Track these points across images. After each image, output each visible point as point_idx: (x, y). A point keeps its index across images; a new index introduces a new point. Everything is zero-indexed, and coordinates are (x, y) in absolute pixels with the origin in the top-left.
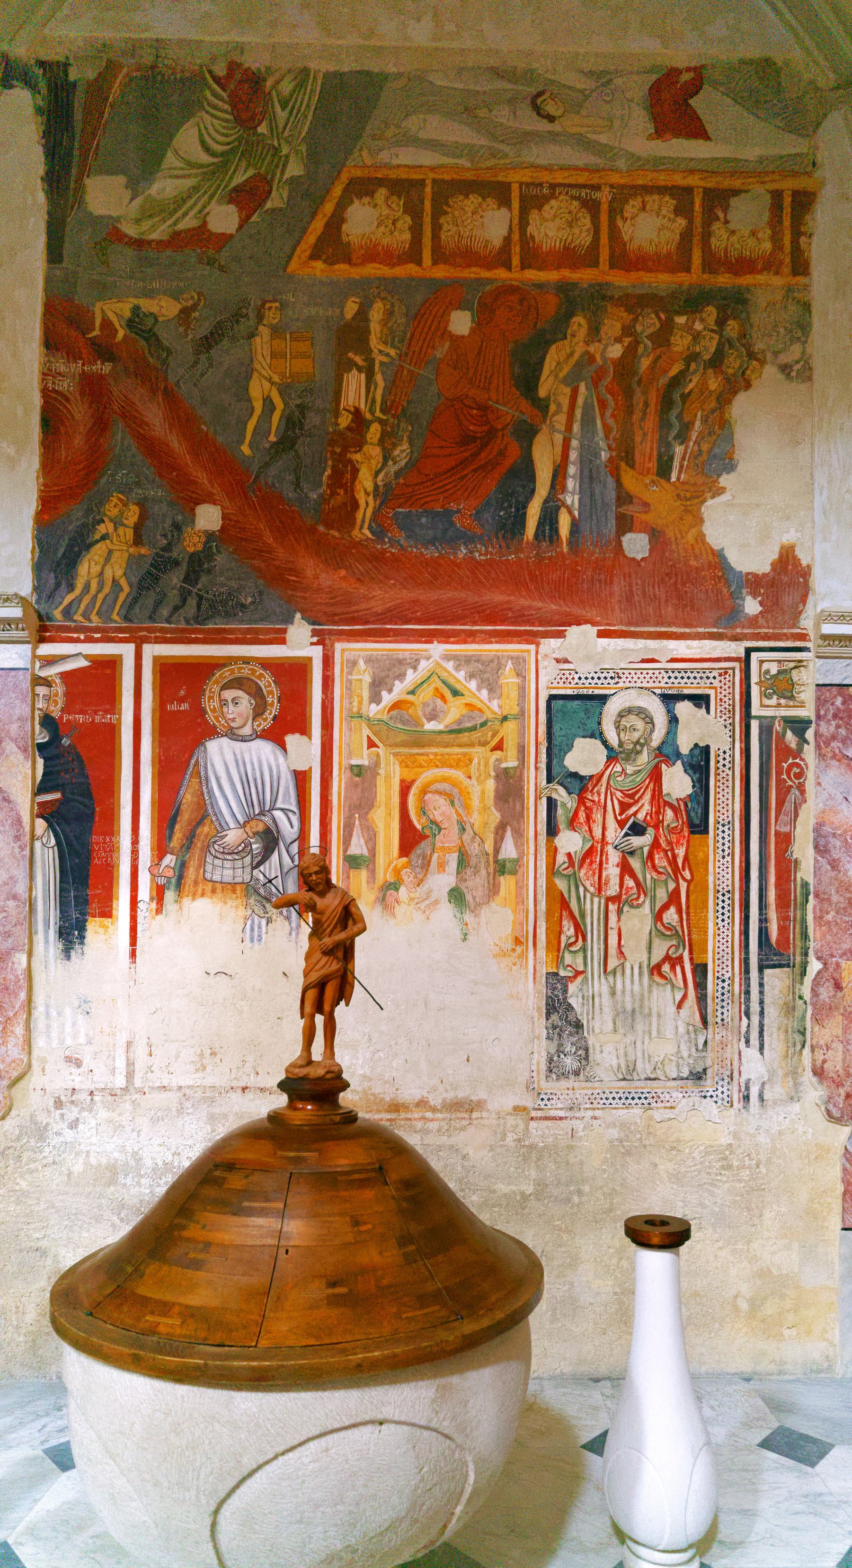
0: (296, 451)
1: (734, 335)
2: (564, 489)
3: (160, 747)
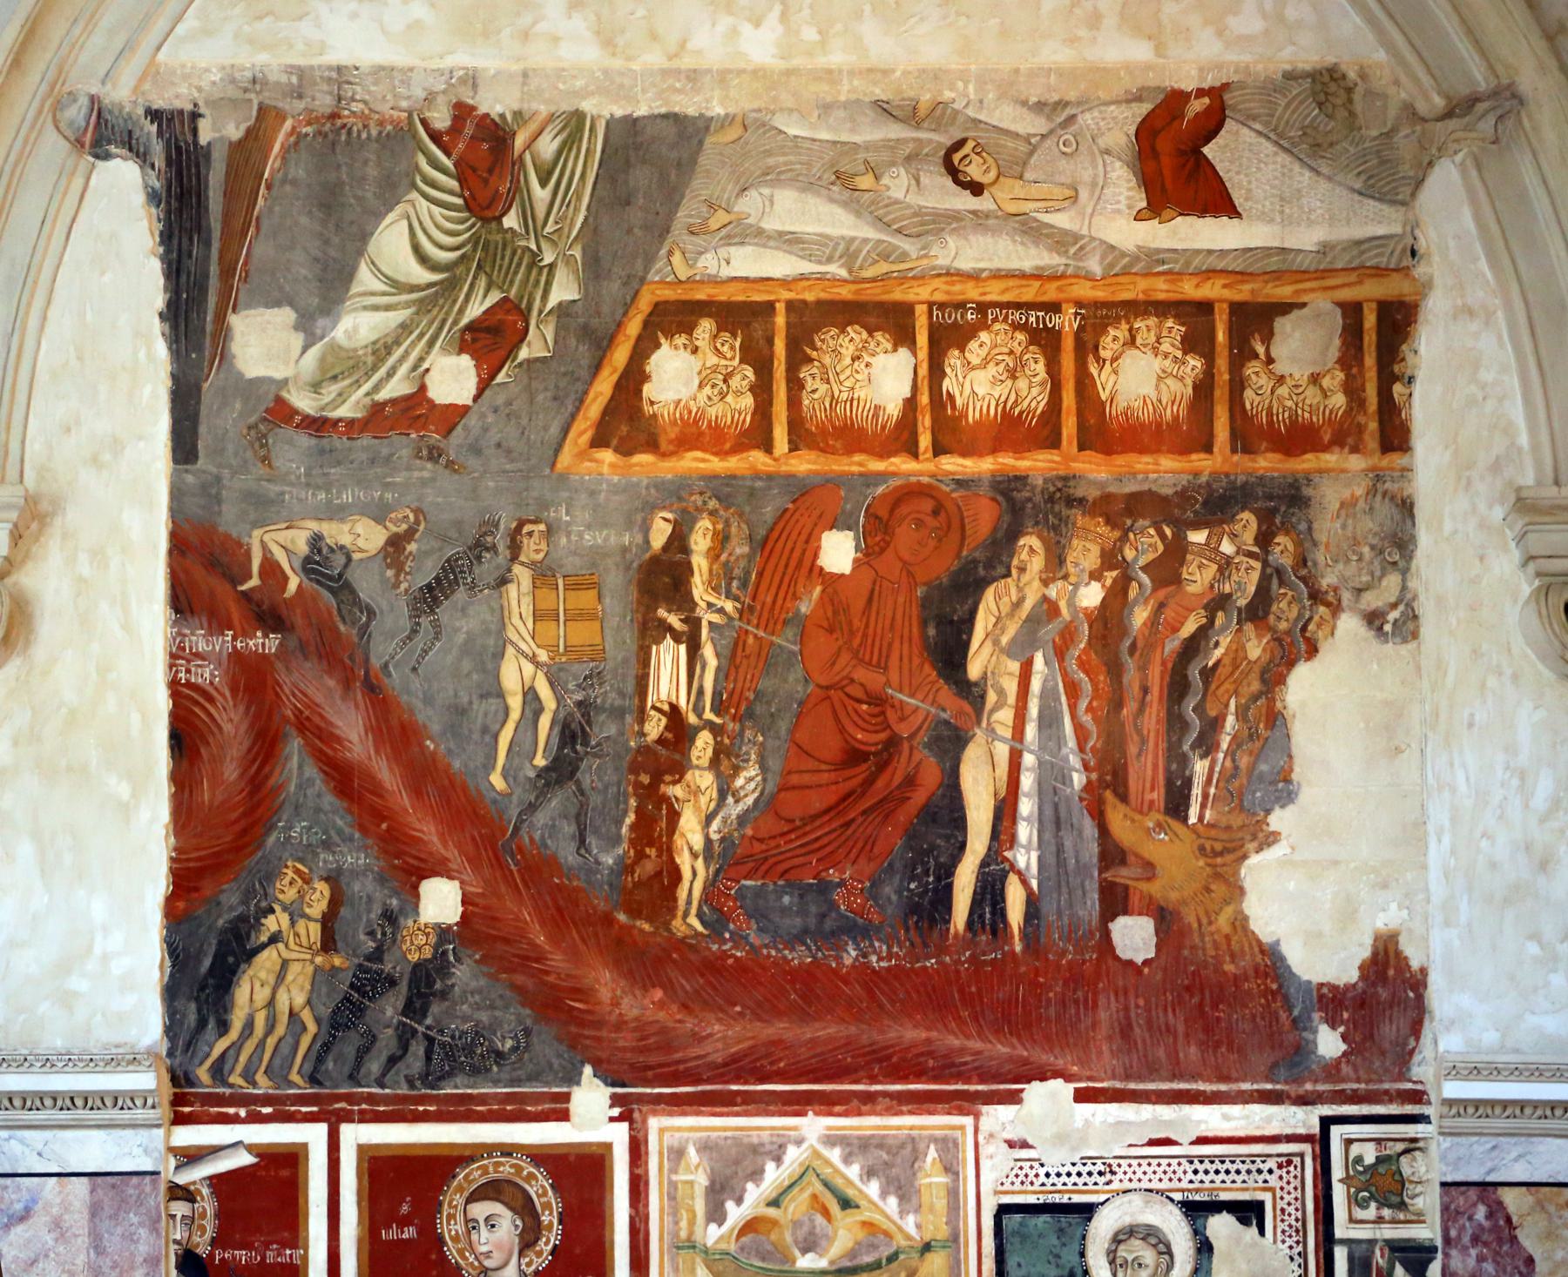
0: (578, 783)
1: (1286, 561)
2: (1012, 841)
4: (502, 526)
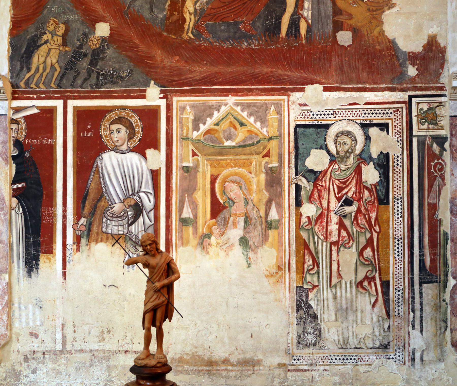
2: (302, 8)
3: (77, 157)
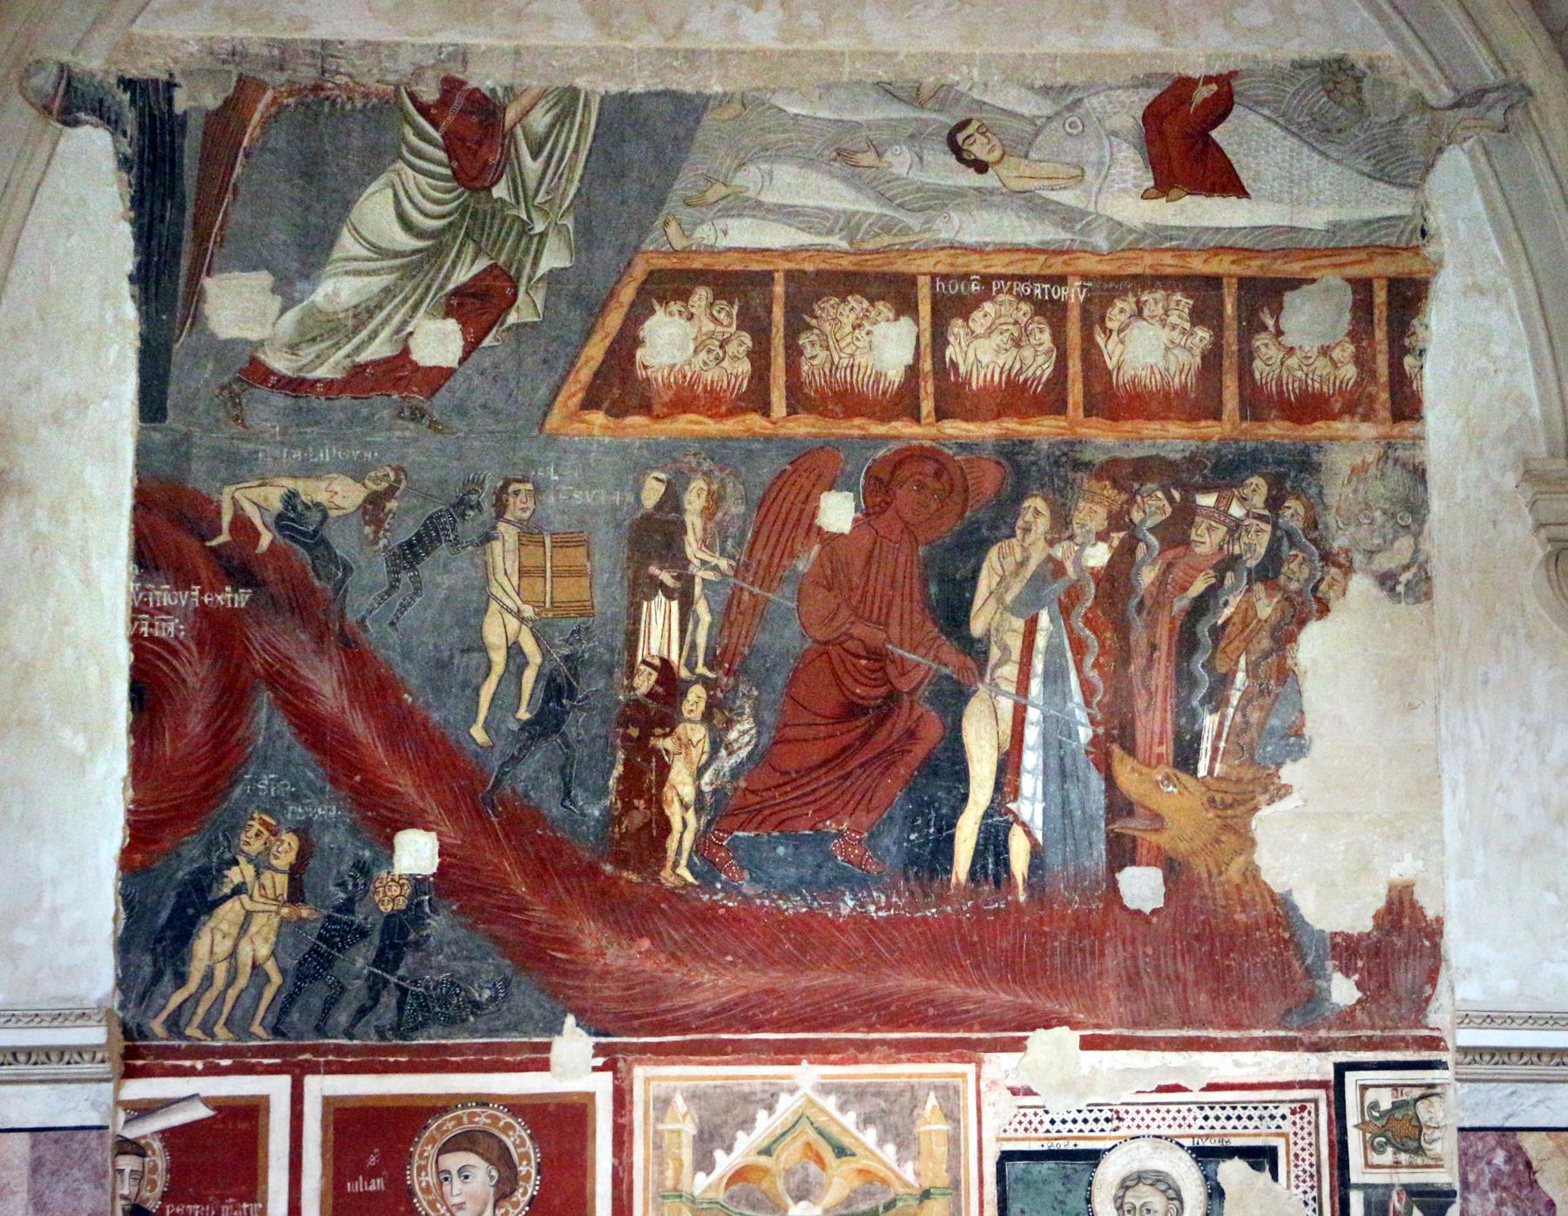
1: (1297, 525)
2: (1016, 792)
4: (487, 486)
